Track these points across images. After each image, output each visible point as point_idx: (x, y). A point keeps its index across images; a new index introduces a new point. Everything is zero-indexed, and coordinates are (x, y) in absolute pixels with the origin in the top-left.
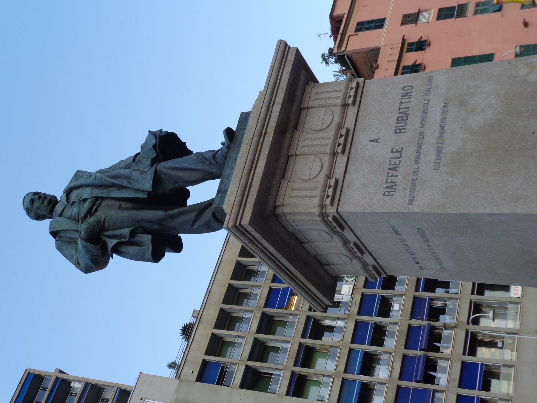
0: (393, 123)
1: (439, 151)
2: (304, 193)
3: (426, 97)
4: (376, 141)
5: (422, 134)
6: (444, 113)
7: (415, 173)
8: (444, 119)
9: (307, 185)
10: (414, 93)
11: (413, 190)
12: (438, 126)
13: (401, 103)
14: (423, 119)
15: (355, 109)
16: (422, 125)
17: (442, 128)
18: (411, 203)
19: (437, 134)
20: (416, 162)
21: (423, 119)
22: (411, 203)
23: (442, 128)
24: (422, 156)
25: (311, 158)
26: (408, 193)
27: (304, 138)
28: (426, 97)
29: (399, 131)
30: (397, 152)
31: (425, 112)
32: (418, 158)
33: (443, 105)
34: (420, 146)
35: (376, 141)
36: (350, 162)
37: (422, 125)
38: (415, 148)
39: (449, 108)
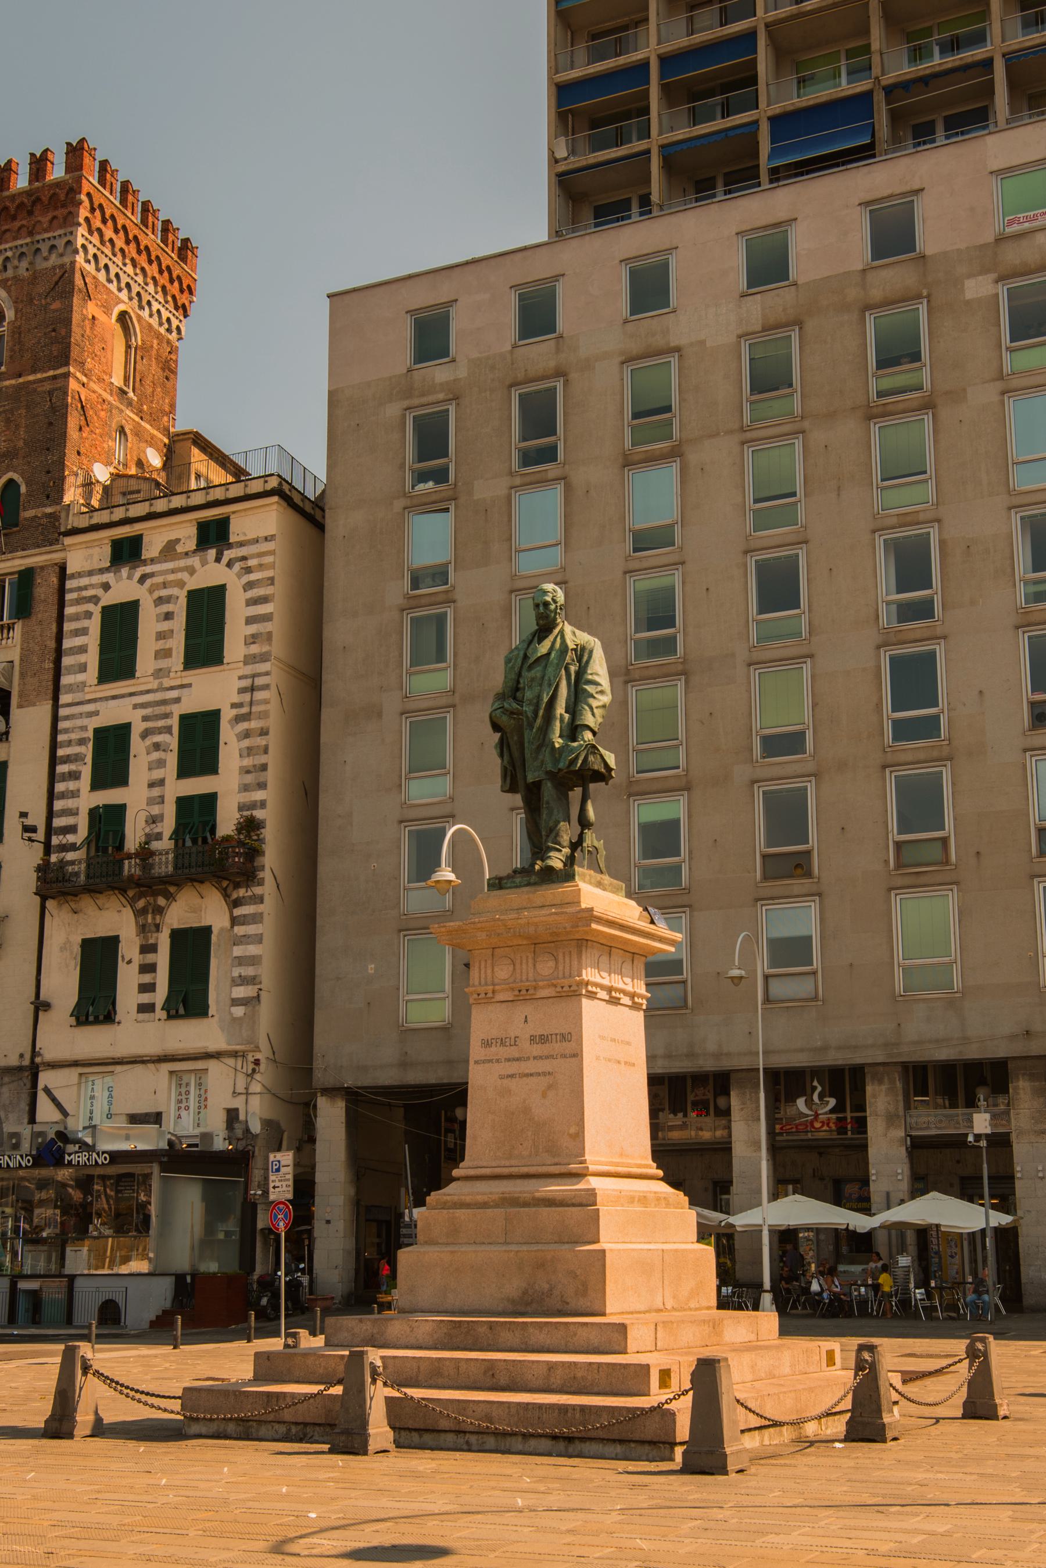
0: (540, 1032)
1: (512, 1076)
2: (483, 972)
3: (559, 1056)
4: (526, 1021)
5: (528, 1058)
6: (544, 1074)
7: (498, 1061)
8: (539, 1074)
9: (489, 971)
10: (564, 1043)
11: (484, 1062)
12: (533, 1071)
13: (556, 1034)
14: (541, 1057)
15: (554, 994)
16: (535, 1058)
17: (531, 1075)
18: (476, 1062)
19: (527, 1071)
20: (505, 1059)
21: (541, 1057)
22: (476, 1062)
23: (531, 1075)
24: (510, 1063)
25: (511, 968)
26: (483, 1058)
27: (529, 954)
28: (559, 1056)
29: (532, 1039)
30: (515, 1041)
31: (547, 1057)
32: (509, 1060)
33: (551, 1071)
34: (518, 1059)
35: (526, 1021)
36: (510, 1003)
37: (535, 1058)
38: (517, 1055)
39: (547, 1077)
